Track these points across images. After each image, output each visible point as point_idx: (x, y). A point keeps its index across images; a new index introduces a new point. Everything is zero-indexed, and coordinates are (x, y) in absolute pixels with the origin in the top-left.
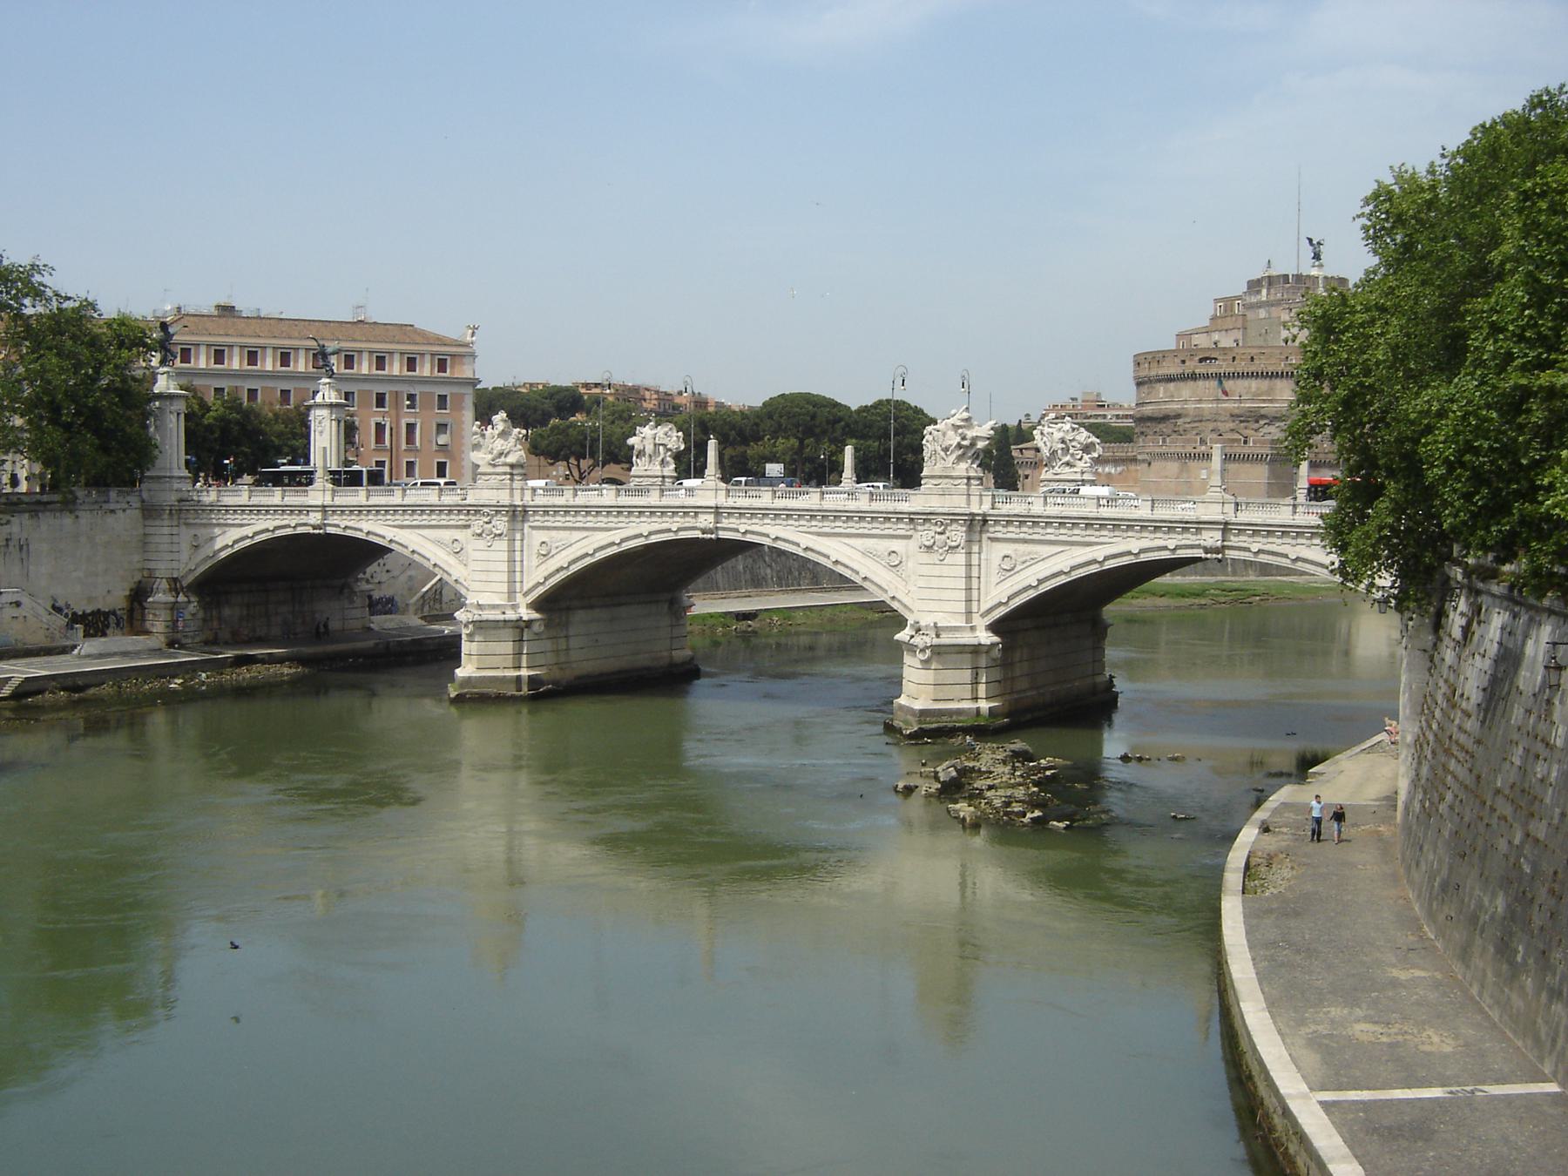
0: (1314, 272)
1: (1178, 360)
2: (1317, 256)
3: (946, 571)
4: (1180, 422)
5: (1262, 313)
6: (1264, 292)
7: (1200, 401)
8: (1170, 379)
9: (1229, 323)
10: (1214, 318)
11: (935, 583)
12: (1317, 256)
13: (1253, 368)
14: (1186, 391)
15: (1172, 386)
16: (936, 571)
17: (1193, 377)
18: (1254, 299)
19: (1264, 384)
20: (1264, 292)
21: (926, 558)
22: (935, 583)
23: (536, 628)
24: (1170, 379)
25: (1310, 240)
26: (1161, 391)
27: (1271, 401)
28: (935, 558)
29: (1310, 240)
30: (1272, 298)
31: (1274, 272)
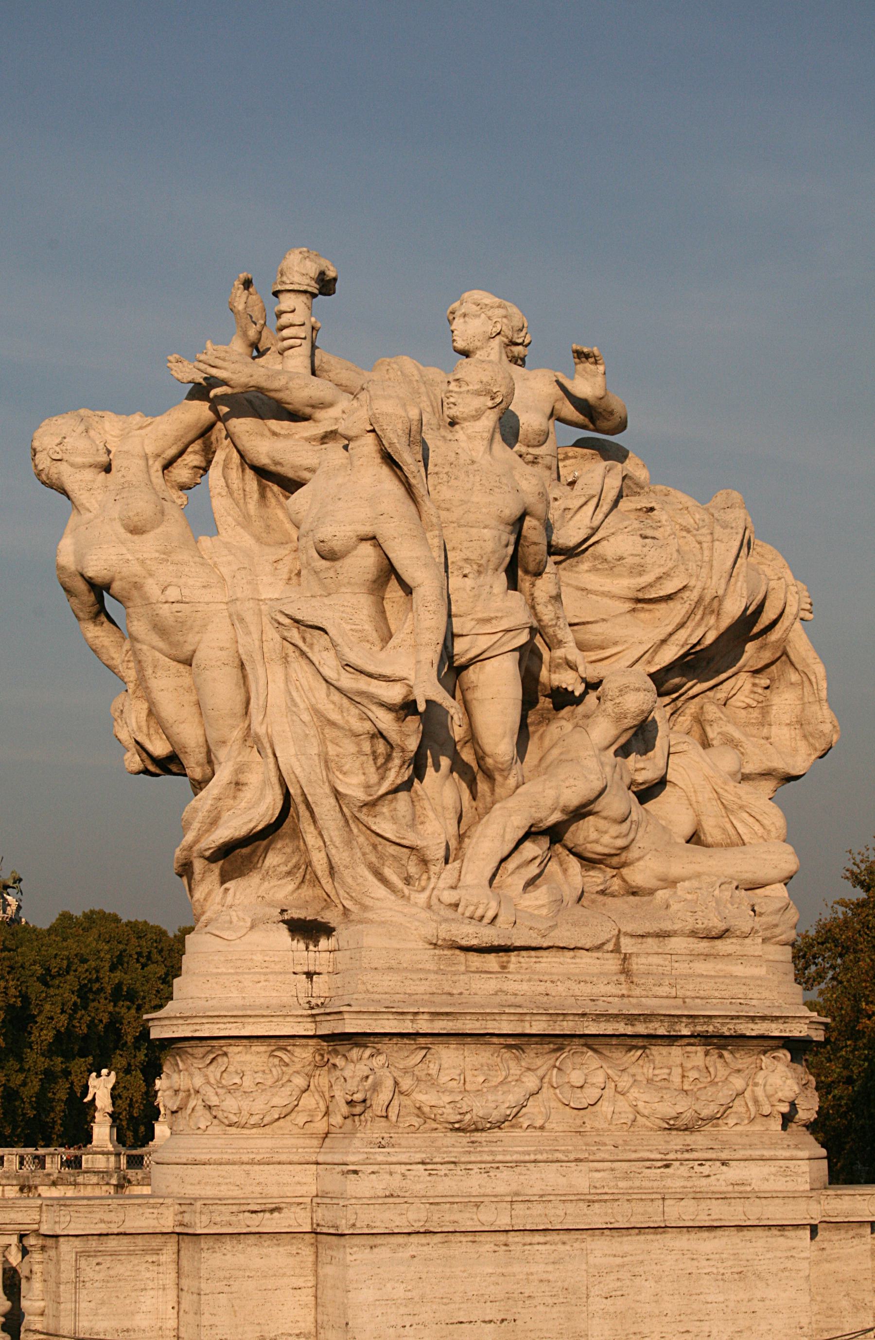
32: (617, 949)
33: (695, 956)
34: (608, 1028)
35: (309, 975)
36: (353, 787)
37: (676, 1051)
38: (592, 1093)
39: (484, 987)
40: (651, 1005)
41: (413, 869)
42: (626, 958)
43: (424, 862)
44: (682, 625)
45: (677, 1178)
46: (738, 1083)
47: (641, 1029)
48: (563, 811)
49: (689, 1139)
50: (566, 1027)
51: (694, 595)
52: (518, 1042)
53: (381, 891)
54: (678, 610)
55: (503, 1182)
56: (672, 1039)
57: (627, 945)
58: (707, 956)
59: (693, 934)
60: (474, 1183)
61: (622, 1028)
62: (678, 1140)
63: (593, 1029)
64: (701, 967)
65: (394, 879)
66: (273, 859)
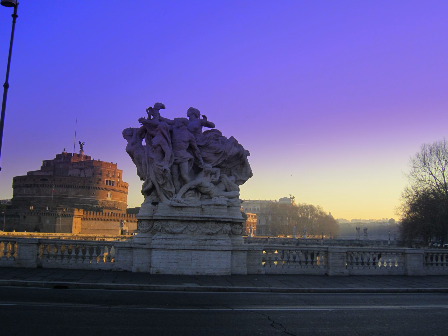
2: (82, 148)
5: (61, 166)
6: (63, 159)
7: (40, 195)
8: (27, 186)
10: (42, 167)
12: (82, 148)
15: (29, 189)
18: (58, 161)
20: (63, 159)
25: (80, 142)
27: (67, 196)
29: (80, 142)
31: (68, 151)
32: (201, 207)
33: (215, 208)
34: (197, 219)
35: (154, 210)
36: (160, 183)
37: (210, 223)
38: (195, 229)
39: (177, 213)
40: (206, 216)
41: (171, 195)
42: (203, 208)
43: (172, 194)
44: (221, 157)
45: (208, 243)
46: (221, 228)
47: (203, 219)
48: (195, 186)
49: (211, 236)
50: (190, 219)
51: (223, 153)
52: (182, 221)
53: (165, 198)
54: (221, 155)
55: (178, 242)
56: (209, 221)
57: (203, 207)
58: (217, 209)
59: (214, 205)
60: (173, 242)
61: (199, 219)
62: (209, 237)
63: (194, 219)
64: (216, 210)
65: (168, 196)
66: (152, 193)
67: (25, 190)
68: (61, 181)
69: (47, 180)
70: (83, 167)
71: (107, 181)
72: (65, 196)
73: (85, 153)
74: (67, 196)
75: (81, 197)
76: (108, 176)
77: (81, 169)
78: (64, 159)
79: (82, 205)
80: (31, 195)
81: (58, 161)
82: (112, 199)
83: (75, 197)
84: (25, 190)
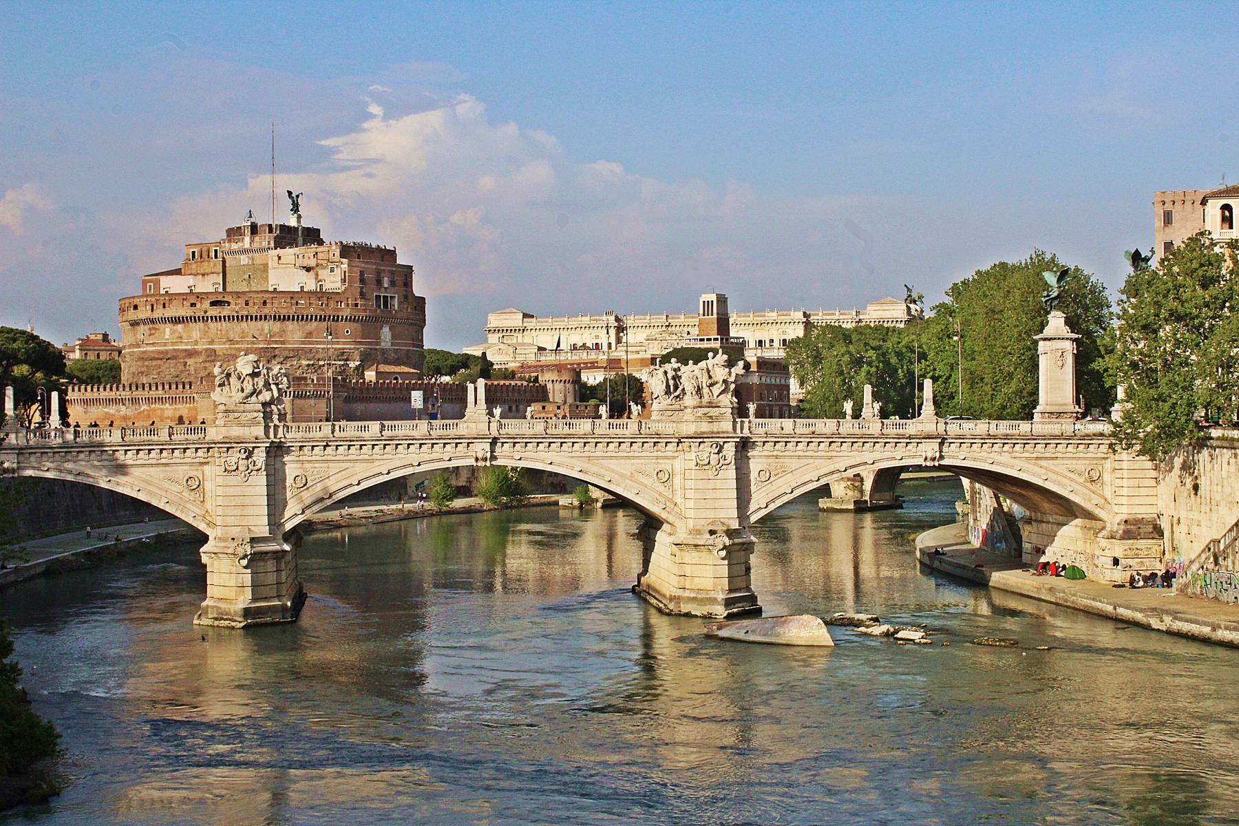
0: (292, 222)
1: (187, 304)
2: (296, 208)
3: (719, 484)
4: (190, 361)
5: (244, 260)
6: (247, 239)
7: (212, 342)
8: (176, 321)
9: (206, 267)
11: (710, 494)
12: (296, 208)
13: (266, 311)
14: (196, 330)
15: (180, 327)
16: (711, 484)
17: (205, 319)
18: (234, 246)
19: (277, 326)
20: (247, 239)
21: (701, 475)
22: (710, 494)
23: (289, 557)
24: (176, 321)
25: (290, 193)
26: (167, 329)
27: (283, 342)
28: (710, 474)
29: (290, 193)
30: (256, 245)
67: (167, 330)
68: (265, 303)
69: (229, 303)
70: (312, 263)
71: (378, 297)
72: (276, 342)
73: (305, 223)
74: (283, 342)
75: (317, 343)
76: (379, 282)
77: (308, 269)
78: (252, 241)
79: (321, 363)
80: (187, 344)
81: (234, 246)
82: (393, 344)
83: (303, 343)
84: (167, 330)
